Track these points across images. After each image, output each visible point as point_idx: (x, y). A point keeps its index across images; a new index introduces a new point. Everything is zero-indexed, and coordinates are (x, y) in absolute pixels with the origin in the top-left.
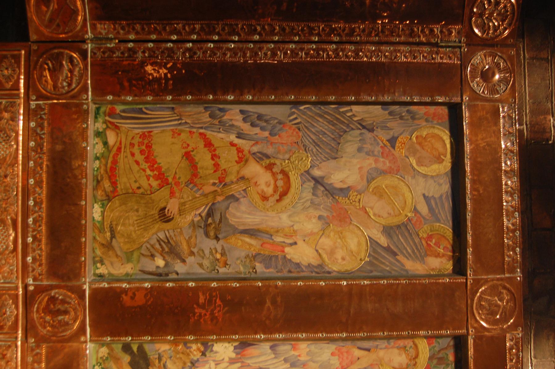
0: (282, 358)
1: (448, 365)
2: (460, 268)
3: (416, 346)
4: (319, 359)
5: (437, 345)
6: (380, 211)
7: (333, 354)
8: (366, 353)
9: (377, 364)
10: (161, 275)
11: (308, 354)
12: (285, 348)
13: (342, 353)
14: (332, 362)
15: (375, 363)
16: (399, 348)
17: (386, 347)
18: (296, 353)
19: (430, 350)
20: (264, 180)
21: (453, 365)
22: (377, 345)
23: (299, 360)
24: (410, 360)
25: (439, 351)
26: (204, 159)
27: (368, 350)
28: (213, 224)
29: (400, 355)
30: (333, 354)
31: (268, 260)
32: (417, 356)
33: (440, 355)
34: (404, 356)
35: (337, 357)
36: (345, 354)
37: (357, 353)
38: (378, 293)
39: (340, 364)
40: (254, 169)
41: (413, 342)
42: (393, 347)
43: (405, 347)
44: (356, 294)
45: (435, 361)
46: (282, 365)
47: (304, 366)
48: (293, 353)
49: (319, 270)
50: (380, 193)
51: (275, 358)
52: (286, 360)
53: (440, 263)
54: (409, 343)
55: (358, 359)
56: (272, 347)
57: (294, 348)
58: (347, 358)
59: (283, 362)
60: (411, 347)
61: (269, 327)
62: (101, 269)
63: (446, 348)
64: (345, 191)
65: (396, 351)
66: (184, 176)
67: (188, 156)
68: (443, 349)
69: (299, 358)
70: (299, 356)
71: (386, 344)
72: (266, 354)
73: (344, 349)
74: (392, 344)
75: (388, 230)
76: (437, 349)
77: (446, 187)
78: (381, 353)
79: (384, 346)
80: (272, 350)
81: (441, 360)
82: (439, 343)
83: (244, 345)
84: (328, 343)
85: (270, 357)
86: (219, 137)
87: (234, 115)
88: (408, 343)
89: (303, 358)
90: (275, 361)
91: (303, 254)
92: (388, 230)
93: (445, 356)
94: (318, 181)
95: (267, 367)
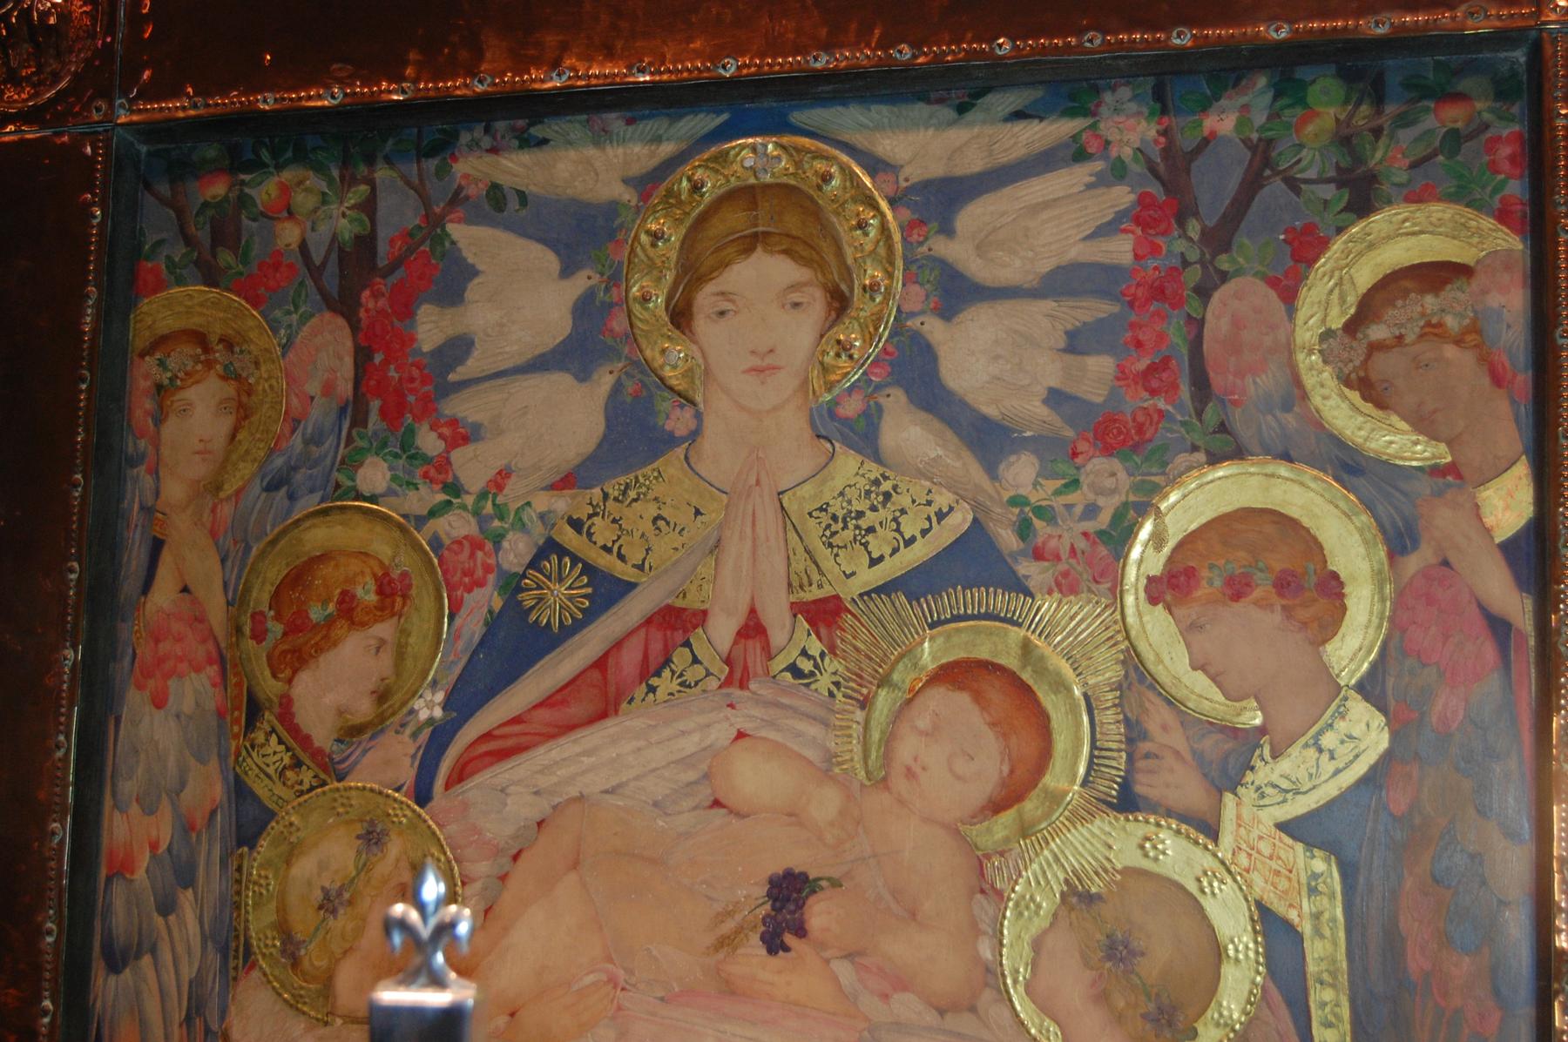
0: (159, 920)
1: (243, 201)
3: (161, 342)
4: (171, 763)
5: (165, 251)
7: (159, 702)
8: (166, 557)
9: (213, 510)
11: (150, 810)
12: (123, 906)
13: (160, 661)
14: (188, 706)
15: (207, 517)
16: (159, 418)
17: (154, 471)
18: (144, 860)
19: (180, 281)
21: (246, 177)
22: (142, 508)
23: (169, 849)
24: (209, 365)
25: (189, 241)
27: (157, 546)
29: (185, 411)
30: (159, 702)
32: (199, 338)
33: (203, 235)
34: (191, 394)
35: (172, 684)
36: (165, 647)
37: (163, 595)
39: (198, 670)
41: (142, 355)
42: (156, 443)
43: (159, 387)
45: (226, 258)
46: (182, 923)
47: (193, 828)
48: (140, 875)
51: (153, 951)
52: (167, 907)
54: (145, 373)
55: (185, 590)
56: (115, 964)
57: (122, 868)
58: (179, 639)
59: (172, 918)
60: (161, 363)
63: (180, 213)
65: (170, 429)
68: (182, 229)
69: (163, 847)
70: (154, 846)
71: (142, 469)
72: (138, 993)
73: (145, 651)
74: (142, 443)
76: (179, 251)
78: (174, 490)
79: (148, 481)
80: (125, 965)
81: (225, 231)
82: (160, 243)
84: (118, 721)
85: (151, 974)
88: (147, 376)
89: (164, 829)
90: (166, 956)
93: (210, 212)
95: (185, 988)
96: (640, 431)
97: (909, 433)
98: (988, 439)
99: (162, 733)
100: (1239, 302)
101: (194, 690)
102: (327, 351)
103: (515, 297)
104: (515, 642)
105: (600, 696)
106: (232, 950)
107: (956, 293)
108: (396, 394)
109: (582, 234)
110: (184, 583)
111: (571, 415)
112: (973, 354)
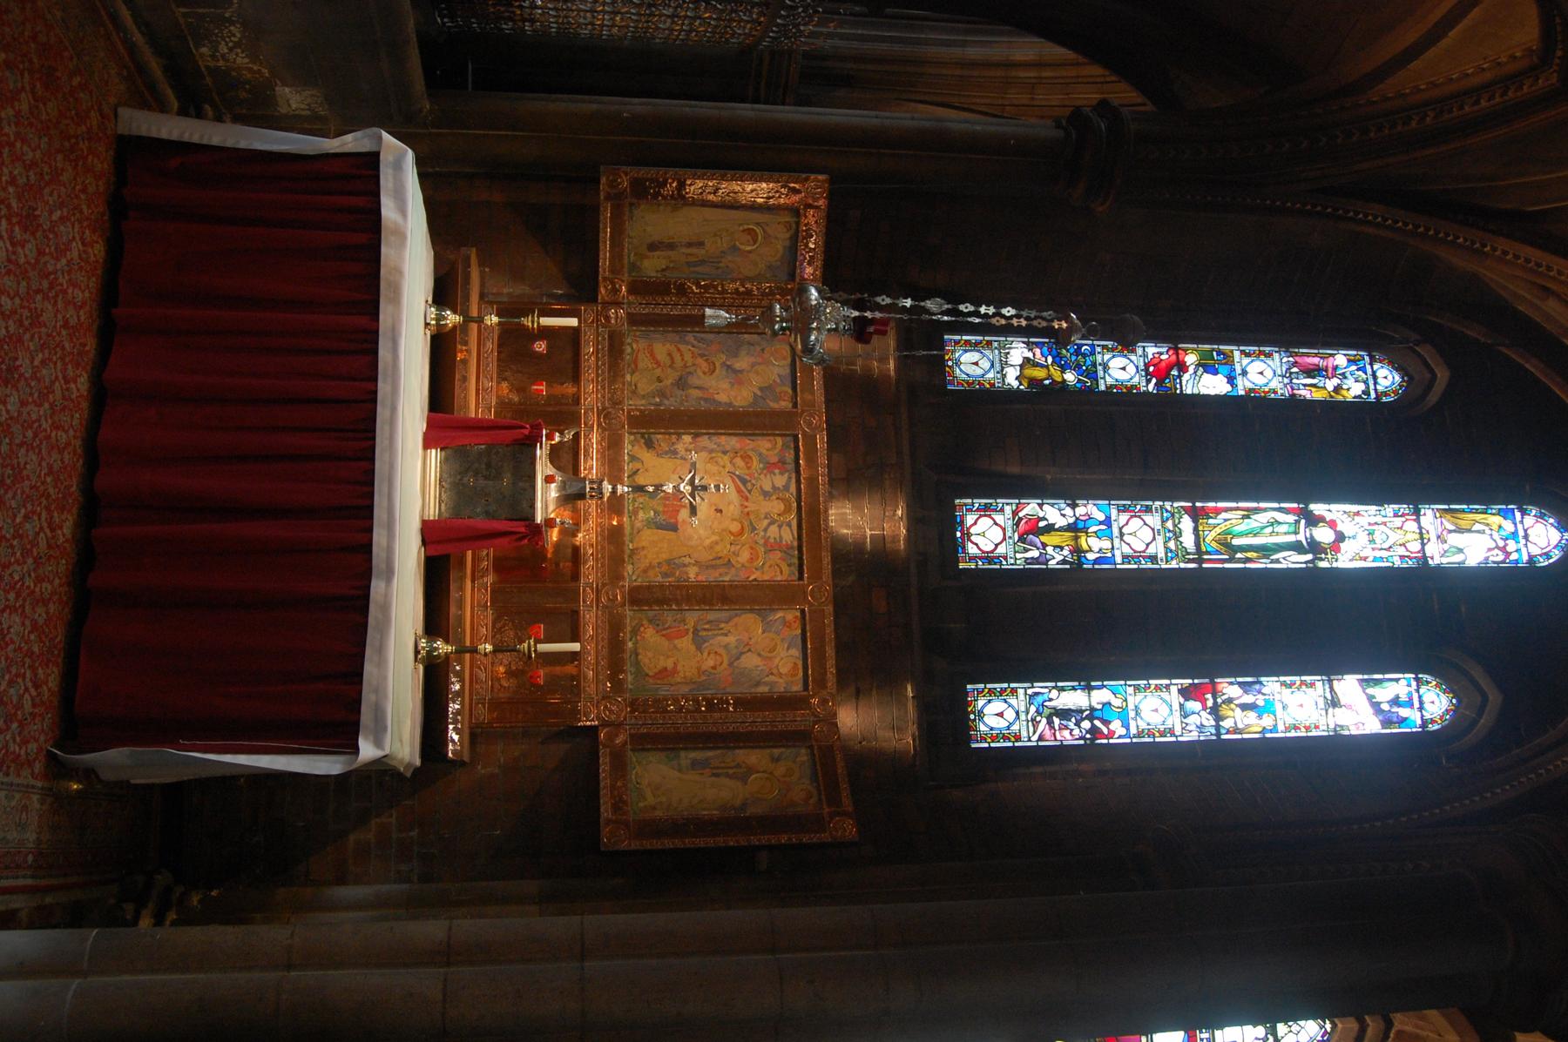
2: (795, 405)
6: (756, 382)
10: (656, 404)
12: (714, 438)
20: (704, 365)
26: (678, 358)
28: (681, 383)
31: (706, 400)
38: (757, 414)
40: (700, 361)
44: (746, 414)
49: (730, 404)
50: (757, 373)
53: (785, 405)
61: (708, 426)
62: (632, 404)
64: (741, 372)
66: (668, 362)
67: (670, 354)
75: (761, 389)
77: (788, 371)
83: (696, 436)
86: (682, 347)
87: (690, 337)
91: (722, 398)
92: (761, 389)
94: (729, 367)
96: (766, 494)
97: (766, 522)
98: (765, 530)
99: (733, 442)
100: (779, 555)
101: (738, 446)
102: (775, 459)
103: (780, 480)
104: (744, 482)
105: (739, 491)
106: (711, 451)
107: (780, 527)
108: (769, 467)
109: (786, 488)
110: (749, 444)
111: (768, 488)
112: (774, 528)
